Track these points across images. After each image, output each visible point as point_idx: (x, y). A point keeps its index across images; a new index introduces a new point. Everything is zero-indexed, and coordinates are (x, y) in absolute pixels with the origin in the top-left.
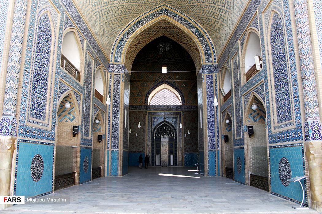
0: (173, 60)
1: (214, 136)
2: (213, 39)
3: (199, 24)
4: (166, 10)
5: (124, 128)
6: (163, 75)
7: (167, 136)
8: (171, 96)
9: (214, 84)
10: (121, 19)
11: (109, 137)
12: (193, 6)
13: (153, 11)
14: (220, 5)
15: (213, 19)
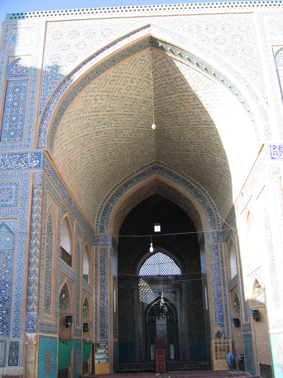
1: (223, 319)
2: (215, 202)
3: (198, 183)
4: (159, 167)
5: (114, 313)
8: (168, 262)
9: (220, 256)
13: (144, 170)
14: (219, 171)
15: (214, 182)
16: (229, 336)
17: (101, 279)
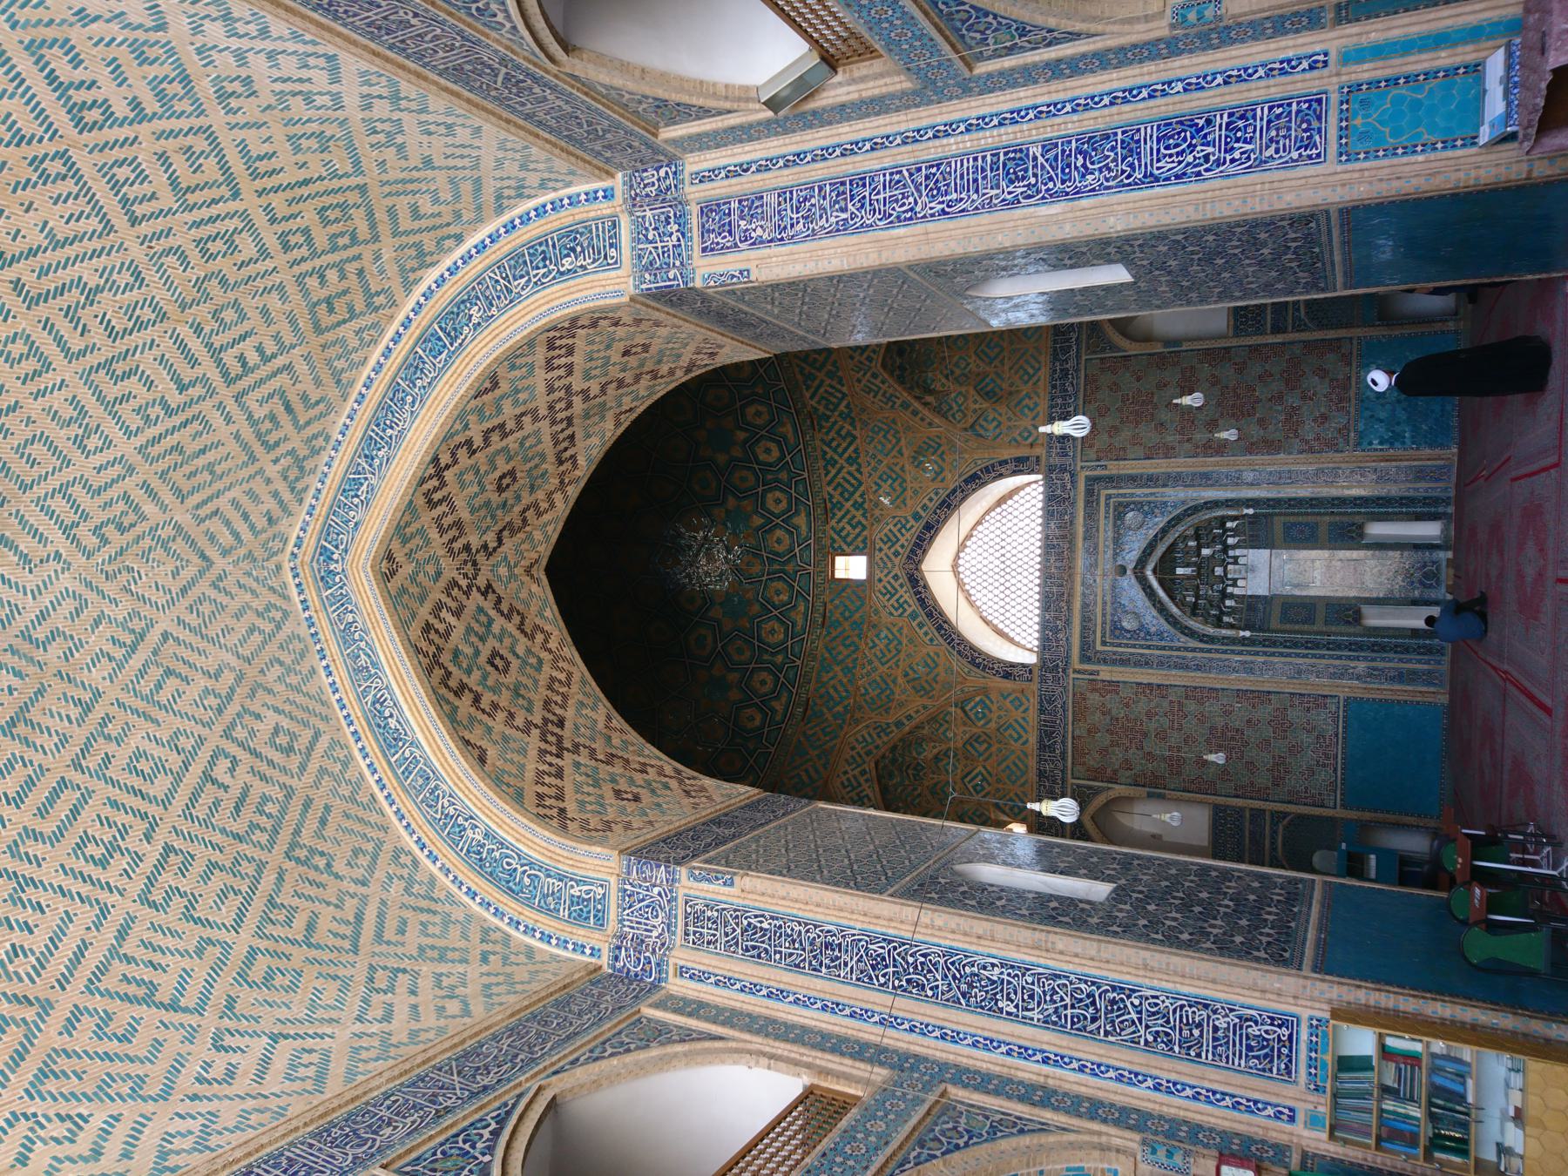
0: (801, 520)
3: (390, 334)
6: (878, 574)
7: (1236, 558)
10: (304, 862)
11: (1173, 1088)
12: (219, 362)
16: (1332, 58)
17: (865, 979)
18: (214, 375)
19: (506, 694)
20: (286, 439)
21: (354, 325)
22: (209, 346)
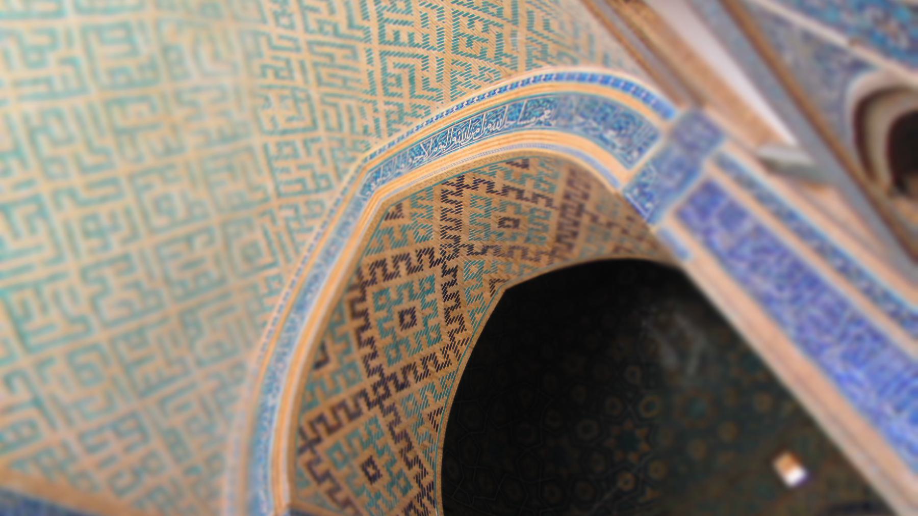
18: (374, 31)
19: (389, 339)
20: (400, 95)
21: (482, 63)
22: (380, 14)
